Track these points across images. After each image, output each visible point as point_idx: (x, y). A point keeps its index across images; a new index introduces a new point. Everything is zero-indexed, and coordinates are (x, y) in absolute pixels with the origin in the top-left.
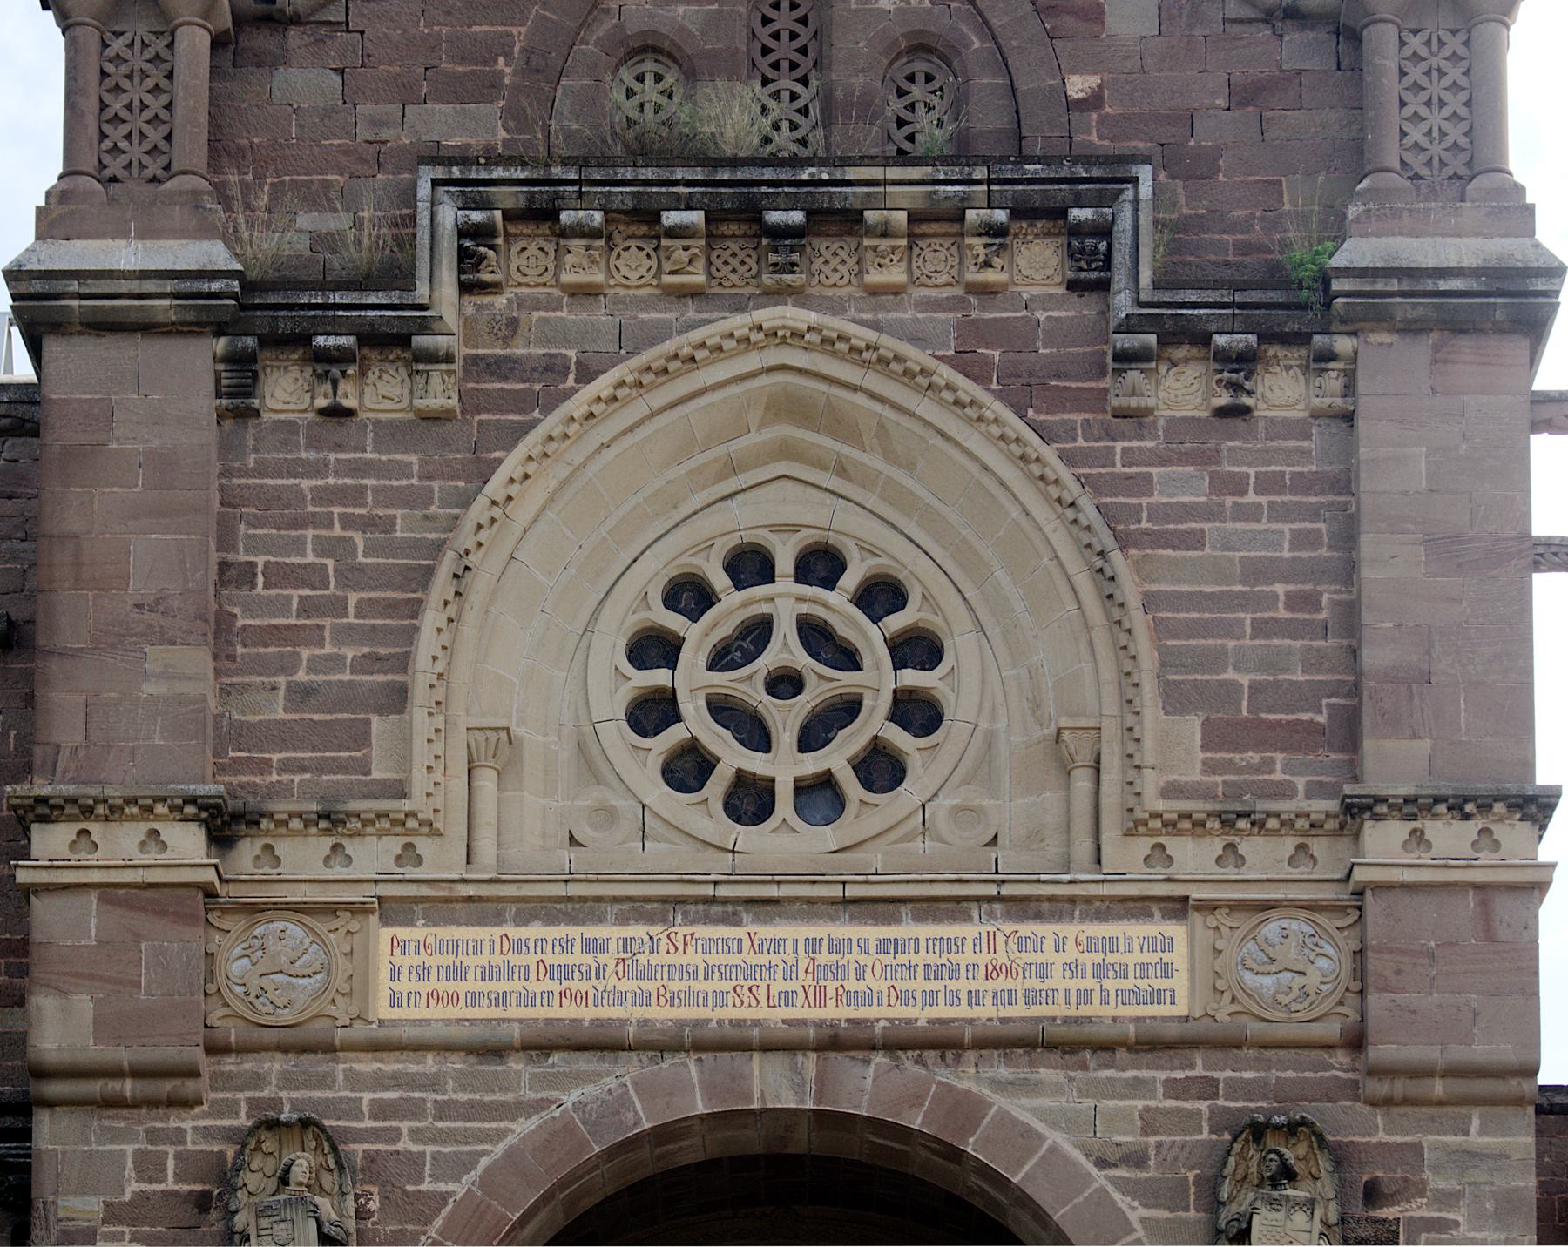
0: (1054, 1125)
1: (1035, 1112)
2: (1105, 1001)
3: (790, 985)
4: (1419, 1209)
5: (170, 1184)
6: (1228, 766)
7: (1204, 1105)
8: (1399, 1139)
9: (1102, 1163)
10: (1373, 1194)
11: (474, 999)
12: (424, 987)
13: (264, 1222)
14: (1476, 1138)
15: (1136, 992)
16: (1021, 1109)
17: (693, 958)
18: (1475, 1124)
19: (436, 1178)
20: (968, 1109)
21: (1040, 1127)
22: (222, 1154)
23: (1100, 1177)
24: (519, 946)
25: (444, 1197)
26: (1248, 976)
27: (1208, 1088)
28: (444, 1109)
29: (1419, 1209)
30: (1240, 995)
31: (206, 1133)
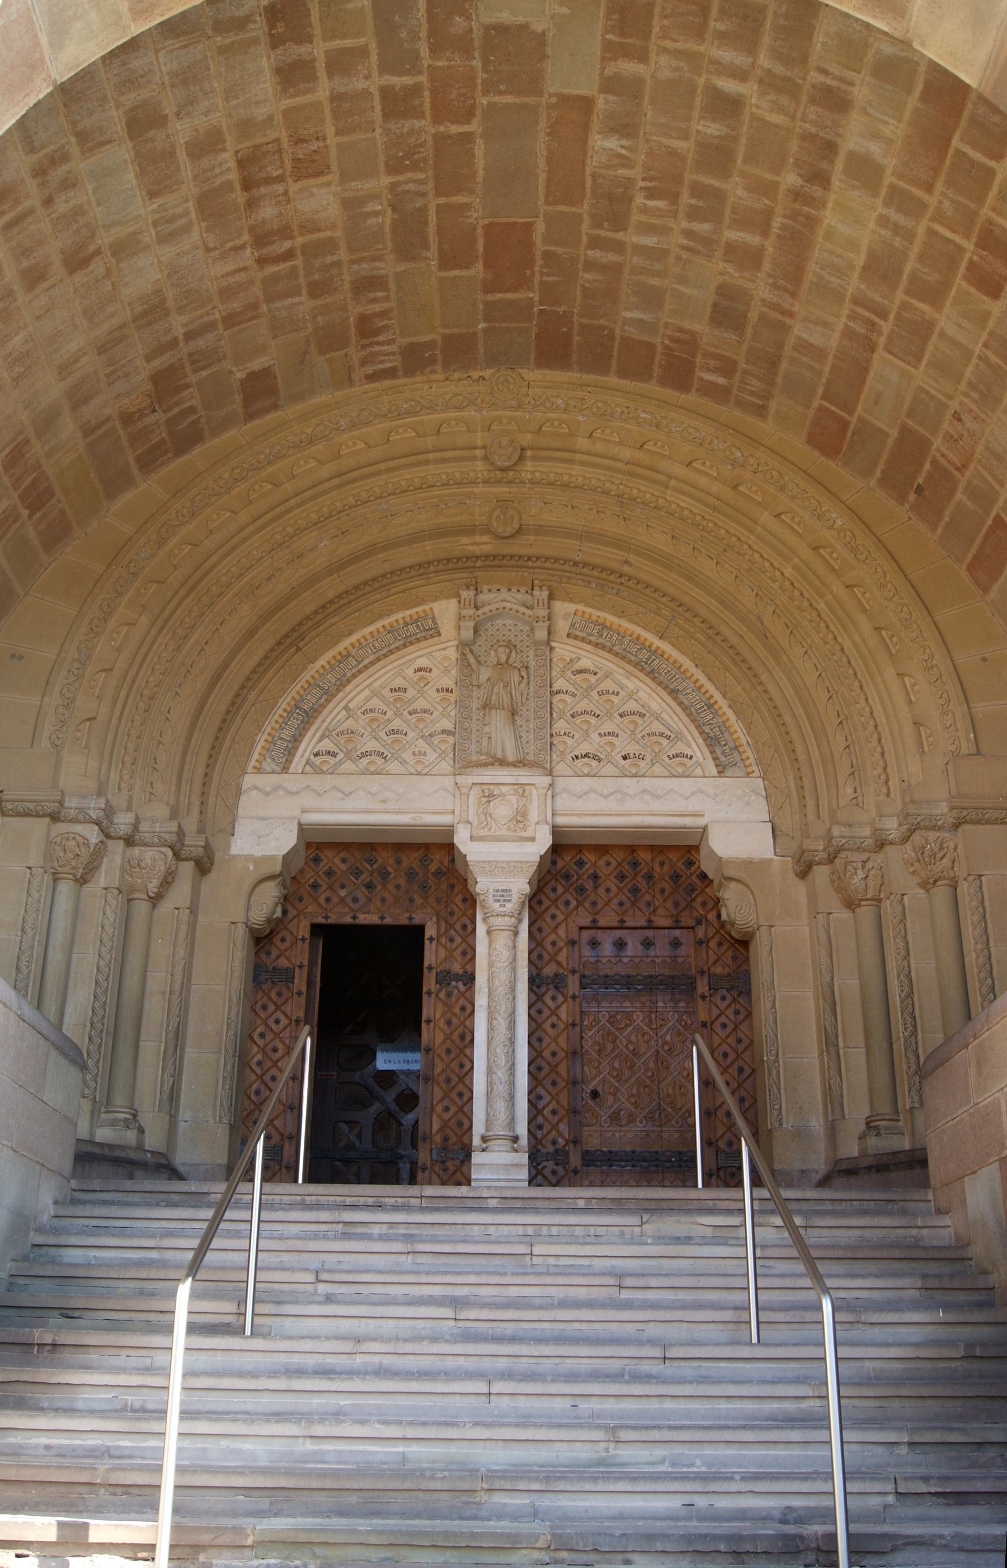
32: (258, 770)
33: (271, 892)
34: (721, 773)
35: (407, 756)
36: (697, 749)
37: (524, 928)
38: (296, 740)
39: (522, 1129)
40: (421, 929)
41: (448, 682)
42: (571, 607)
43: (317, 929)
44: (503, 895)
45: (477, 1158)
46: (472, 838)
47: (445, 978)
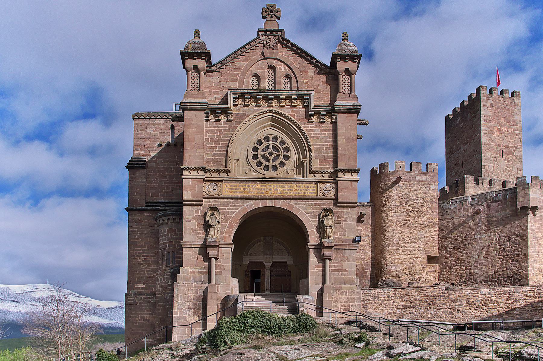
0: (302, 209)
1: (300, 207)
2: (308, 194)
3: (271, 191)
4: (343, 219)
5: (199, 215)
6: (322, 165)
7: (319, 206)
8: (341, 211)
9: (307, 214)
10: (338, 218)
11: (234, 192)
12: (229, 191)
13: (211, 219)
14: (350, 211)
15: (311, 192)
16: (298, 207)
17: (260, 188)
18: (350, 209)
19: (230, 214)
20: (292, 207)
21: (300, 209)
22: (205, 211)
23: (307, 215)
24: (240, 186)
25: (231, 216)
26: (324, 191)
27: (319, 204)
28: (231, 206)
29: (343, 219)
30: (323, 193)
31: (203, 208)
32: (245, 255)
33: (246, 267)
34: (289, 255)
35: (259, 254)
36: (286, 253)
37: (270, 271)
38: (248, 252)
39: (270, 289)
40: (260, 270)
41: (262, 246)
42: (275, 238)
43: (250, 270)
44: (268, 268)
45: (266, 291)
46: (265, 263)
47: (263, 275)
